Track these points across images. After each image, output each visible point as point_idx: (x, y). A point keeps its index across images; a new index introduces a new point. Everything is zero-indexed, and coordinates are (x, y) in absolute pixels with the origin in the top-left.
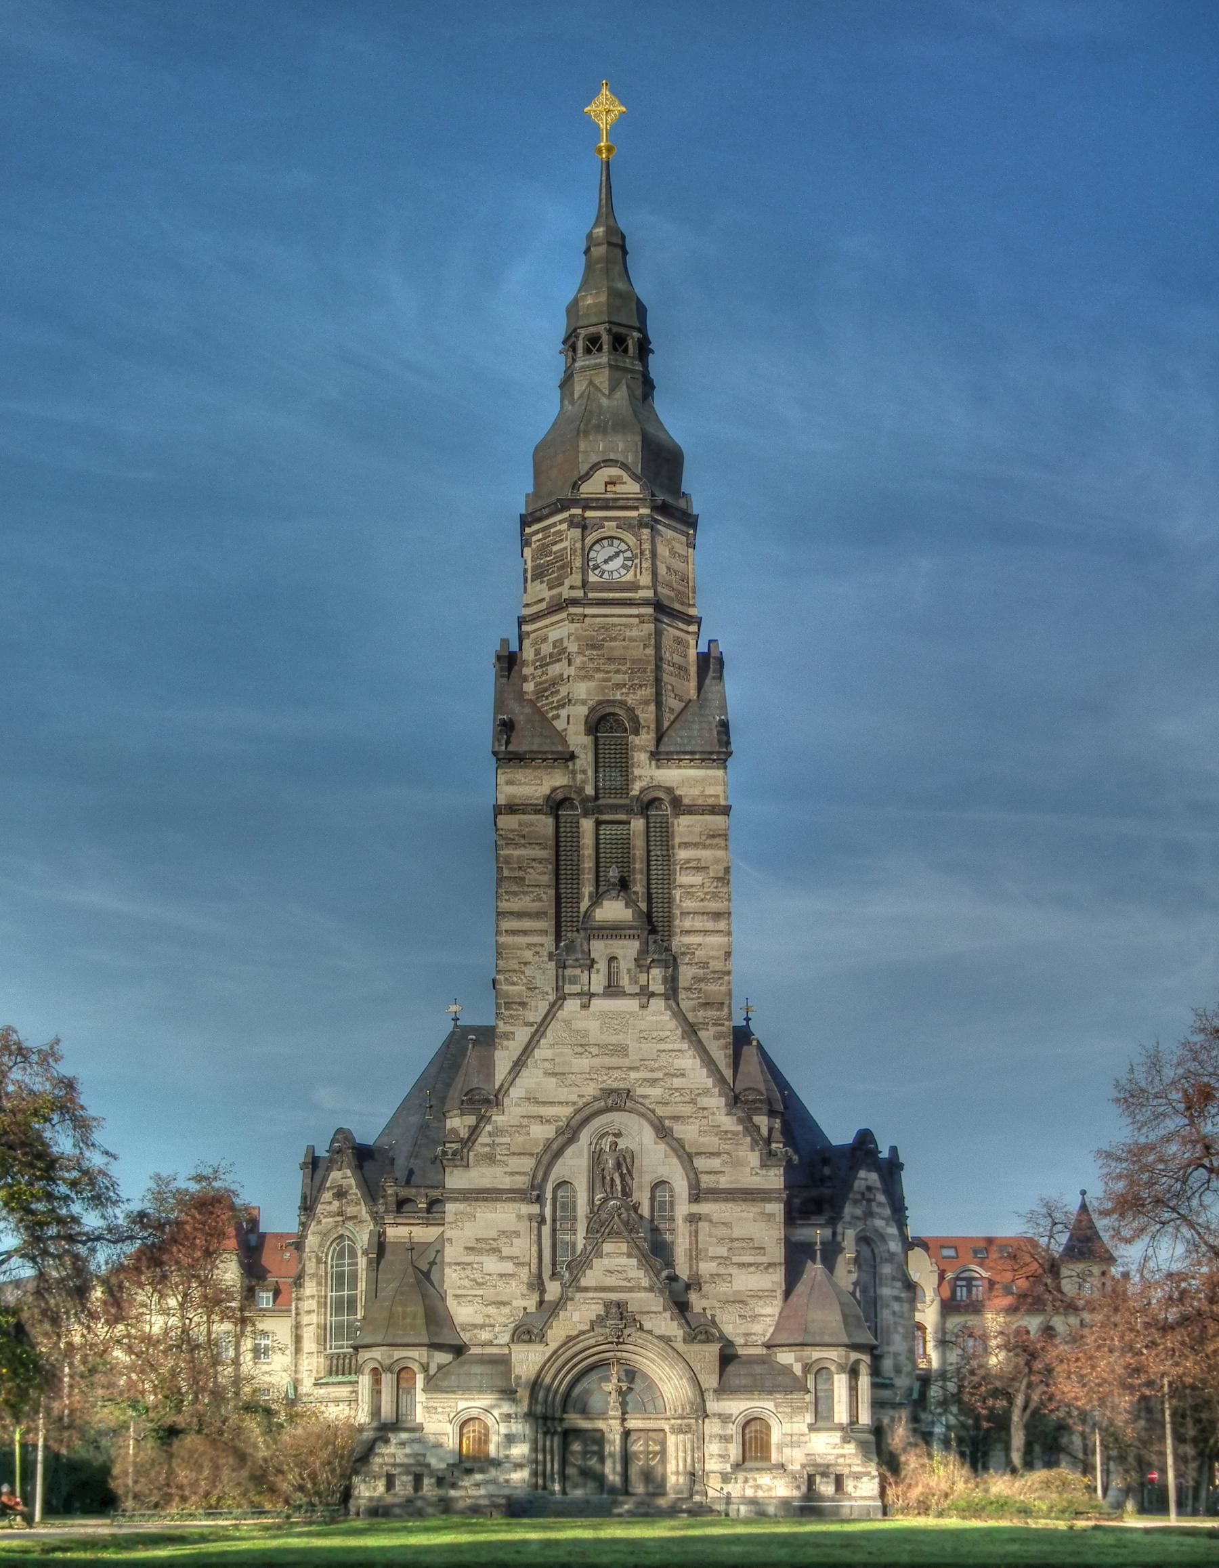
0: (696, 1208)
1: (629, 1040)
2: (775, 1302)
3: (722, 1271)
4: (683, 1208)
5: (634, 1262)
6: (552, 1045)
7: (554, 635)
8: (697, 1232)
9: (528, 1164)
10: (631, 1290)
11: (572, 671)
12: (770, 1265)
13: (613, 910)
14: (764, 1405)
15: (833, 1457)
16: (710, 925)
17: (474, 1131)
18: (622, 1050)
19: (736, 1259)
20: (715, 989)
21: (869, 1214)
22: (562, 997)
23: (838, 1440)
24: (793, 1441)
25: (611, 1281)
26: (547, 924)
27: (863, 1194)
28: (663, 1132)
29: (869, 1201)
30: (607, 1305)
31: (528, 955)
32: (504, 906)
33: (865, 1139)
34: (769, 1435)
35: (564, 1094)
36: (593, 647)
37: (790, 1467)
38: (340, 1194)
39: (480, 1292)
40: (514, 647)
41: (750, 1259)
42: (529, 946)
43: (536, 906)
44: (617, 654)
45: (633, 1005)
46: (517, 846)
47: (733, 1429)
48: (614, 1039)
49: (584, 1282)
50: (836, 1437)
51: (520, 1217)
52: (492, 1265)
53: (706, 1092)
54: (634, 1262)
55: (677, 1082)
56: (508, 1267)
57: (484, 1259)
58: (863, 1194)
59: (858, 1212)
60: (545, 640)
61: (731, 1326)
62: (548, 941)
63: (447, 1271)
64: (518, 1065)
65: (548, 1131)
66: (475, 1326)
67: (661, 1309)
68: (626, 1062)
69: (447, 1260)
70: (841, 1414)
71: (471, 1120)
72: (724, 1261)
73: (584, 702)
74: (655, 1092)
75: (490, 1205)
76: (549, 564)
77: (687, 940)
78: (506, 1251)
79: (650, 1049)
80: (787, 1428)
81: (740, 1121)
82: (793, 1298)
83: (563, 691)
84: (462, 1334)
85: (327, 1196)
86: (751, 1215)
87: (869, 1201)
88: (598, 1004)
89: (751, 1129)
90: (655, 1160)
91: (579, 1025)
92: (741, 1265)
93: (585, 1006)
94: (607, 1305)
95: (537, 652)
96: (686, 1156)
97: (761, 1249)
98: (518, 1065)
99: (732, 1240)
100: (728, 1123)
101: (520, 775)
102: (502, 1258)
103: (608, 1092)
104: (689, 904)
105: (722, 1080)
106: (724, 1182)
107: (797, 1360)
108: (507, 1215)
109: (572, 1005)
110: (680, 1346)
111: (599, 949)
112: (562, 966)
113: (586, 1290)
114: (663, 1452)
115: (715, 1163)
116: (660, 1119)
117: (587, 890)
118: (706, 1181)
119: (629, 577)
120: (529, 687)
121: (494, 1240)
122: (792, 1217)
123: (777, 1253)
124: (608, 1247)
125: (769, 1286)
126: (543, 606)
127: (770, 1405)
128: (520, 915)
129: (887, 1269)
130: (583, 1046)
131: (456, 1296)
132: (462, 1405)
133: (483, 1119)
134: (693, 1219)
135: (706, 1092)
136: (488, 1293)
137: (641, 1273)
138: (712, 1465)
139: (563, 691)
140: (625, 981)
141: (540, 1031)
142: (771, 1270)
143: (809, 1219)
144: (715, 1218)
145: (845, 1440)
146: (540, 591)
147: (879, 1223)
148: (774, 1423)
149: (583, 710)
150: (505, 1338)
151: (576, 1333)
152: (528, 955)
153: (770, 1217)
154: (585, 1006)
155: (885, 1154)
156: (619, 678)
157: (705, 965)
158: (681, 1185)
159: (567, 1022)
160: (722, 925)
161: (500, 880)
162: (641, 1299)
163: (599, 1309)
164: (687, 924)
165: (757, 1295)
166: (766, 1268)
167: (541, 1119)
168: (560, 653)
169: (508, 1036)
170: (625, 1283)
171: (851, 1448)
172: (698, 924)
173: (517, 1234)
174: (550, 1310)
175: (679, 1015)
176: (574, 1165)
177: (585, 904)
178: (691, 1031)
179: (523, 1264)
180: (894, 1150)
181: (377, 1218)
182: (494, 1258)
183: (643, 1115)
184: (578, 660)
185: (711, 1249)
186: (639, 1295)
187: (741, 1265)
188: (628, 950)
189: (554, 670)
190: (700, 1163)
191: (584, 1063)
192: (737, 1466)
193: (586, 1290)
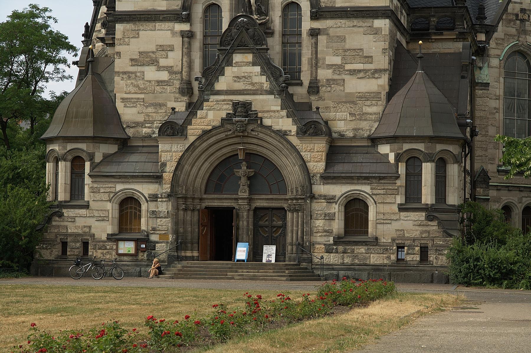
0: (317, 25)
2: (380, 103)
3: (336, 77)
4: (307, 24)
5: (258, 69)
8: (316, 44)
10: (254, 93)
12: (376, 71)
15: (418, 232)
19: (348, 67)
23: (423, 218)
24: (382, 221)
27: (517, 15)
29: (522, 21)
30: (235, 105)
34: (367, 213)
39: (142, 96)
41: (360, 66)
47: (336, 209)
50: (421, 216)
51: (174, 33)
52: (151, 74)
54: (258, 69)
56: (164, 76)
57: (146, 69)
58: (517, 15)
59: (513, 31)
61: (342, 124)
63: (117, 79)
67: (279, 108)
69: (116, 69)
70: (428, 196)
72: (337, 68)
75: (151, 25)
78: (163, 62)
80: (382, 208)
82: (394, 99)
84: (127, 130)
86: (361, 29)
87: (522, 21)
92: (353, 72)
94: (235, 105)
97: (369, 59)
99: (346, 51)
102: (160, 68)
107: (391, 151)
108: (165, 34)
110: (294, 140)
113: (218, 93)
114: (284, 226)
121: (153, 52)
123: (382, 61)
124: (237, 58)
127: (367, 188)
131: (122, 99)
132: (119, 187)
134: (314, 33)
136: (149, 98)
137: (264, 78)
138: (319, 238)
142: (376, 75)
143: (442, 34)
144: (331, 32)
145: (429, 218)
151: (210, 128)
153: (377, 32)
162: (263, 100)
163: (227, 109)
165: (365, 97)
166: (373, 74)
170: (250, 87)
171: (433, 226)
173: (171, 48)
174: (193, 108)
179: (176, 73)
182: (153, 68)
185: (327, 58)
186: (261, 97)
187: (353, 72)
192: (338, 240)
193: (218, 93)
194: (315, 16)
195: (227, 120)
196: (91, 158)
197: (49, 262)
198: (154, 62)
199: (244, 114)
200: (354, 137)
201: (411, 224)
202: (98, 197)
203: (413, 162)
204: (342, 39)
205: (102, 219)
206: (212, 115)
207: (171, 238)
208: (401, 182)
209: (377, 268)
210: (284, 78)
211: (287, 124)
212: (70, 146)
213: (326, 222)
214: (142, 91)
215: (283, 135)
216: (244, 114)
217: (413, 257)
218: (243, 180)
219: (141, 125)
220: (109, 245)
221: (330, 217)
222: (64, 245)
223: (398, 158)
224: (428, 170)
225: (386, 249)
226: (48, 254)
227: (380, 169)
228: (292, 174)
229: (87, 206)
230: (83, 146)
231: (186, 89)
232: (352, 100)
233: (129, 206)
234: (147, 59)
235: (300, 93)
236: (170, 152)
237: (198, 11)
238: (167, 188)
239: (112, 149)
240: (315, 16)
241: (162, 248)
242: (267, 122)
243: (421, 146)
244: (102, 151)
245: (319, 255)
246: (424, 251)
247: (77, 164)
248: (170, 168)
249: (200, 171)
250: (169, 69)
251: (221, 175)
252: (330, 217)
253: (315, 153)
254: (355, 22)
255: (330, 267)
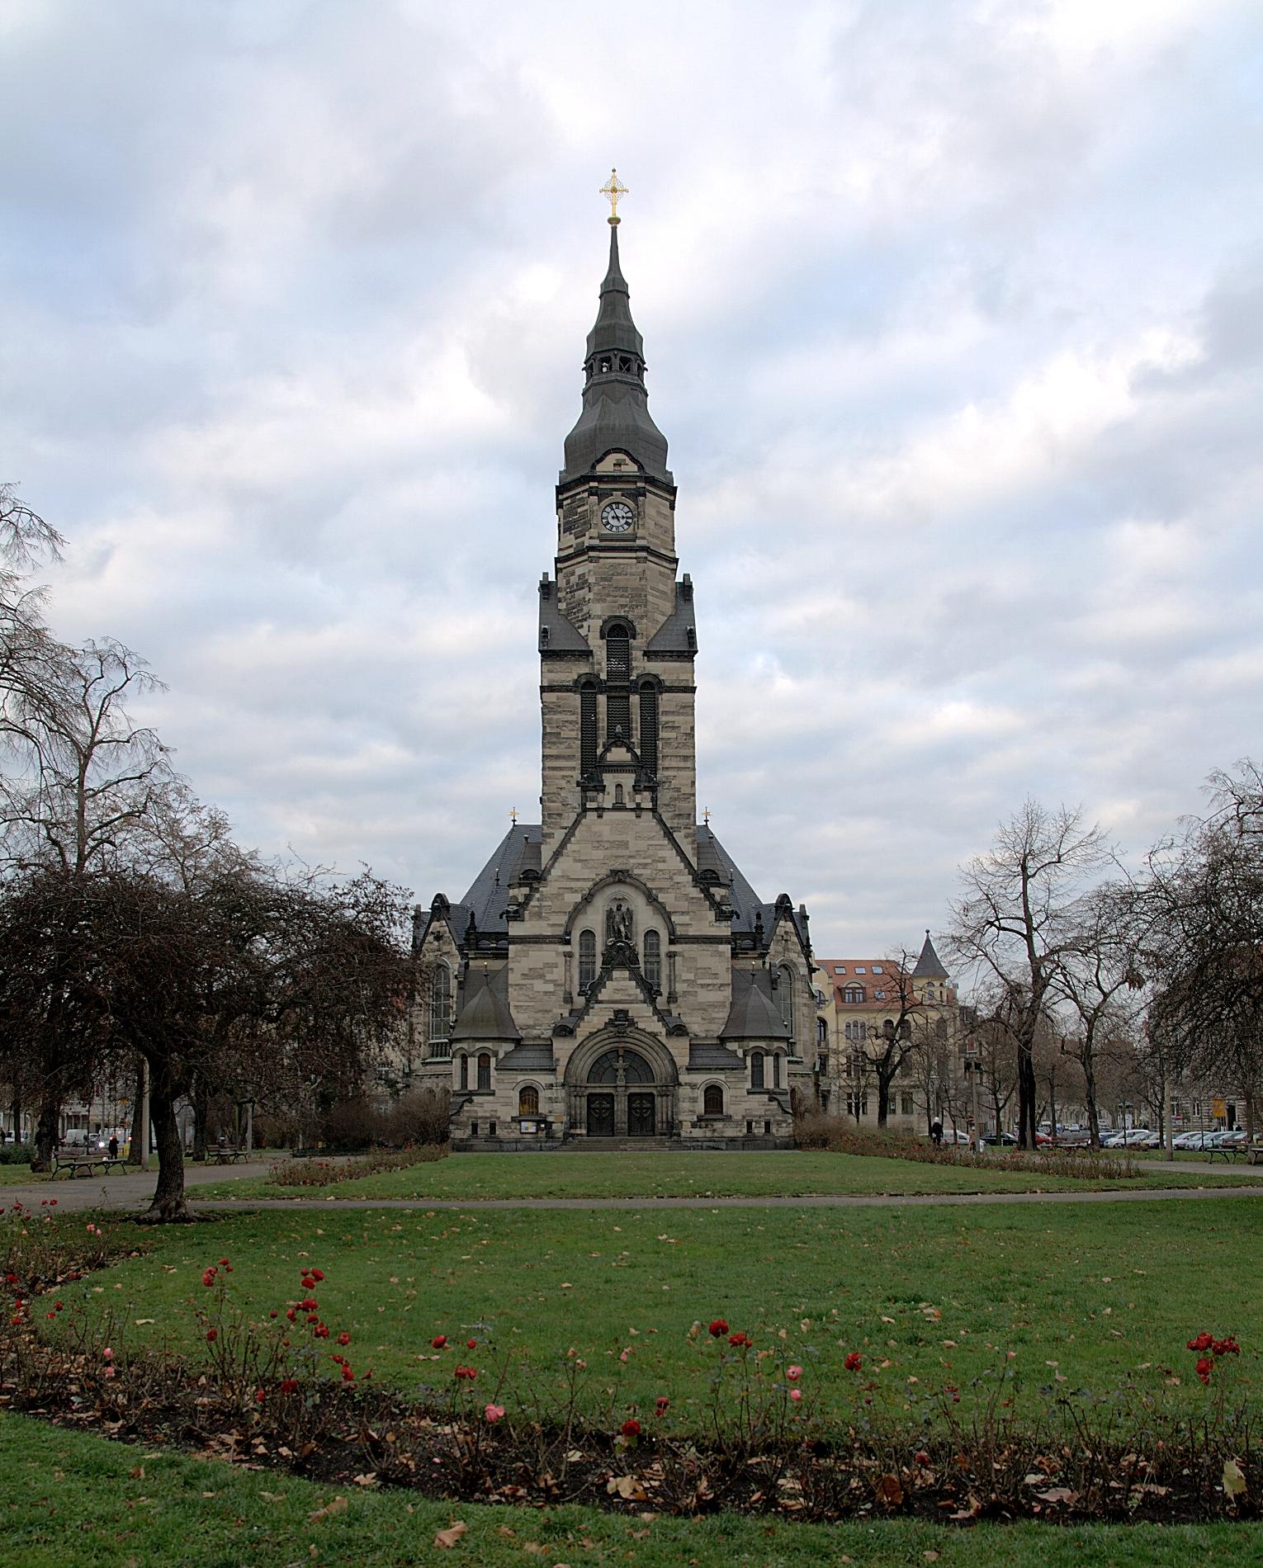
0: (673, 948)
1: (629, 837)
4: (665, 947)
6: (578, 842)
7: (579, 571)
9: (564, 919)
10: (631, 1002)
11: (591, 596)
13: (619, 754)
14: (719, 1078)
16: (682, 764)
17: (528, 898)
18: (625, 845)
20: (683, 806)
21: (786, 949)
22: (585, 810)
24: (736, 1101)
25: (617, 997)
26: (577, 763)
28: (651, 899)
31: (563, 783)
32: (548, 752)
33: (784, 899)
35: (587, 874)
36: (605, 579)
37: (735, 1118)
38: (438, 937)
40: (552, 578)
42: (563, 777)
43: (569, 752)
44: (621, 584)
45: (633, 814)
46: (555, 713)
47: (700, 1094)
48: (619, 838)
49: (600, 997)
51: (558, 954)
52: (539, 986)
53: (680, 872)
55: (661, 866)
56: (550, 988)
60: (573, 574)
61: (695, 1025)
62: (577, 775)
64: (557, 854)
65: (578, 898)
66: (529, 1027)
68: (626, 853)
70: (769, 1084)
71: (526, 890)
73: (599, 617)
74: (646, 872)
76: (575, 521)
77: (667, 773)
78: (549, 977)
79: (642, 845)
81: (702, 891)
83: (585, 609)
85: (430, 938)
88: (606, 815)
89: (709, 897)
90: (645, 919)
91: (595, 828)
93: (600, 816)
94: (617, 1012)
95: (568, 582)
96: (667, 916)
98: (557, 854)
100: (695, 893)
101: (559, 665)
102: (546, 982)
103: (614, 873)
104: (667, 751)
105: (688, 865)
106: (692, 932)
109: (592, 816)
110: (663, 1039)
111: (609, 779)
112: (584, 790)
114: (653, 1108)
115: (685, 919)
116: (650, 890)
117: (601, 741)
118: (679, 931)
119: (630, 530)
120: (562, 606)
122: (734, 955)
123: (727, 978)
124: (616, 974)
125: (721, 999)
126: (571, 551)
127: (722, 1077)
128: (557, 757)
129: (799, 985)
130: (599, 844)
132: (520, 1078)
133: (534, 890)
134: (671, 955)
135: (680, 872)
139: (585, 609)
140: (626, 800)
141: (571, 832)
146: (570, 539)
147: (793, 956)
148: (725, 1088)
149: (600, 622)
150: (549, 1033)
152: (563, 783)
153: (721, 954)
154: (600, 816)
155: (796, 910)
156: (623, 601)
157: (678, 790)
158: (664, 935)
159: (589, 827)
160: (689, 764)
161: (544, 734)
164: (667, 764)
165: (713, 1005)
167: (572, 890)
168: (583, 583)
169: (551, 835)
172: (674, 764)
174: (579, 1015)
175: (661, 822)
176: (594, 919)
177: (599, 751)
178: (669, 834)
180: (802, 907)
181: (464, 956)
183: (637, 887)
184: (595, 589)
187: (702, 986)
188: (628, 780)
189: (579, 594)
190: (673, 918)
191: (599, 854)
192: (700, 1119)
194: (672, 942)
195: (611, 1022)
196: (496, 1054)
197: (462, 1140)
198: (542, 976)
199: (621, 1020)
200: (706, 1038)
201: (757, 1105)
202: (502, 1086)
203: (758, 1056)
204: (694, 959)
205: (507, 1104)
206: (597, 1018)
207: (565, 1119)
208: (749, 1072)
209: (732, 1140)
210: (650, 992)
211: (657, 1027)
212: (479, 1045)
213: (690, 1104)
214: (532, 999)
215: (654, 1035)
216: (621, 1020)
217: (759, 1130)
218: (621, 1072)
219: (533, 1027)
220: (514, 1125)
221: (694, 1100)
222: (475, 1127)
223: (745, 1056)
224: (769, 1062)
225: (738, 1124)
226: (458, 1134)
227: (733, 1061)
228: (660, 1067)
229: (493, 1094)
230: (489, 1045)
231: (568, 999)
232: (703, 1008)
233: (528, 1095)
234: (535, 974)
235: (661, 1001)
236: (563, 1048)
237: (576, 936)
238: (561, 1080)
239: (510, 1047)
240: (672, 942)
241: (558, 1128)
242: (641, 1026)
243: (763, 1044)
244: (505, 1048)
245: (686, 1131)
246: (768, 1124)
247: (484, 1059)
248: (563, 1062)
249: (584, 1064)
250: (553, 981)
251: (600, 1068)
252: (694, 1100)
253: (680, 1050)
254: (704, 946)
255: (695, 1140)
